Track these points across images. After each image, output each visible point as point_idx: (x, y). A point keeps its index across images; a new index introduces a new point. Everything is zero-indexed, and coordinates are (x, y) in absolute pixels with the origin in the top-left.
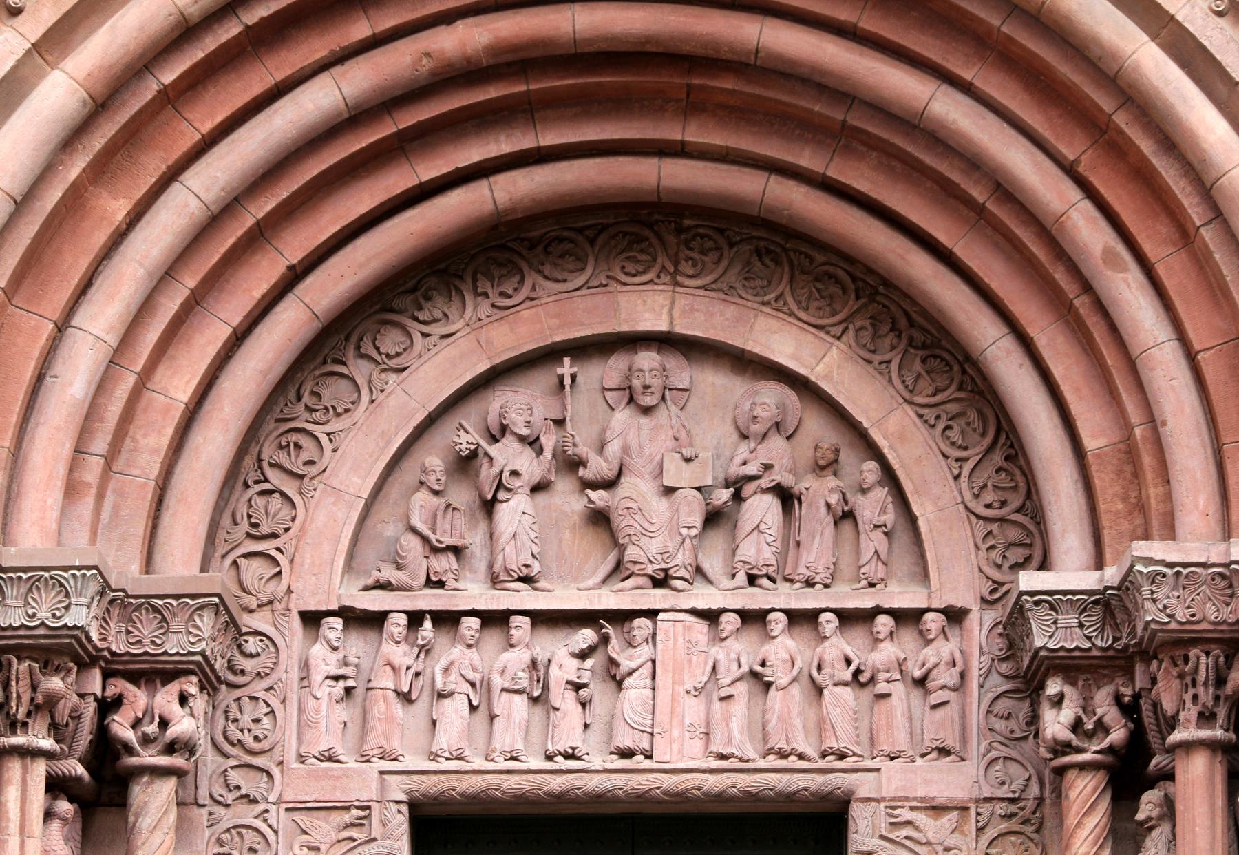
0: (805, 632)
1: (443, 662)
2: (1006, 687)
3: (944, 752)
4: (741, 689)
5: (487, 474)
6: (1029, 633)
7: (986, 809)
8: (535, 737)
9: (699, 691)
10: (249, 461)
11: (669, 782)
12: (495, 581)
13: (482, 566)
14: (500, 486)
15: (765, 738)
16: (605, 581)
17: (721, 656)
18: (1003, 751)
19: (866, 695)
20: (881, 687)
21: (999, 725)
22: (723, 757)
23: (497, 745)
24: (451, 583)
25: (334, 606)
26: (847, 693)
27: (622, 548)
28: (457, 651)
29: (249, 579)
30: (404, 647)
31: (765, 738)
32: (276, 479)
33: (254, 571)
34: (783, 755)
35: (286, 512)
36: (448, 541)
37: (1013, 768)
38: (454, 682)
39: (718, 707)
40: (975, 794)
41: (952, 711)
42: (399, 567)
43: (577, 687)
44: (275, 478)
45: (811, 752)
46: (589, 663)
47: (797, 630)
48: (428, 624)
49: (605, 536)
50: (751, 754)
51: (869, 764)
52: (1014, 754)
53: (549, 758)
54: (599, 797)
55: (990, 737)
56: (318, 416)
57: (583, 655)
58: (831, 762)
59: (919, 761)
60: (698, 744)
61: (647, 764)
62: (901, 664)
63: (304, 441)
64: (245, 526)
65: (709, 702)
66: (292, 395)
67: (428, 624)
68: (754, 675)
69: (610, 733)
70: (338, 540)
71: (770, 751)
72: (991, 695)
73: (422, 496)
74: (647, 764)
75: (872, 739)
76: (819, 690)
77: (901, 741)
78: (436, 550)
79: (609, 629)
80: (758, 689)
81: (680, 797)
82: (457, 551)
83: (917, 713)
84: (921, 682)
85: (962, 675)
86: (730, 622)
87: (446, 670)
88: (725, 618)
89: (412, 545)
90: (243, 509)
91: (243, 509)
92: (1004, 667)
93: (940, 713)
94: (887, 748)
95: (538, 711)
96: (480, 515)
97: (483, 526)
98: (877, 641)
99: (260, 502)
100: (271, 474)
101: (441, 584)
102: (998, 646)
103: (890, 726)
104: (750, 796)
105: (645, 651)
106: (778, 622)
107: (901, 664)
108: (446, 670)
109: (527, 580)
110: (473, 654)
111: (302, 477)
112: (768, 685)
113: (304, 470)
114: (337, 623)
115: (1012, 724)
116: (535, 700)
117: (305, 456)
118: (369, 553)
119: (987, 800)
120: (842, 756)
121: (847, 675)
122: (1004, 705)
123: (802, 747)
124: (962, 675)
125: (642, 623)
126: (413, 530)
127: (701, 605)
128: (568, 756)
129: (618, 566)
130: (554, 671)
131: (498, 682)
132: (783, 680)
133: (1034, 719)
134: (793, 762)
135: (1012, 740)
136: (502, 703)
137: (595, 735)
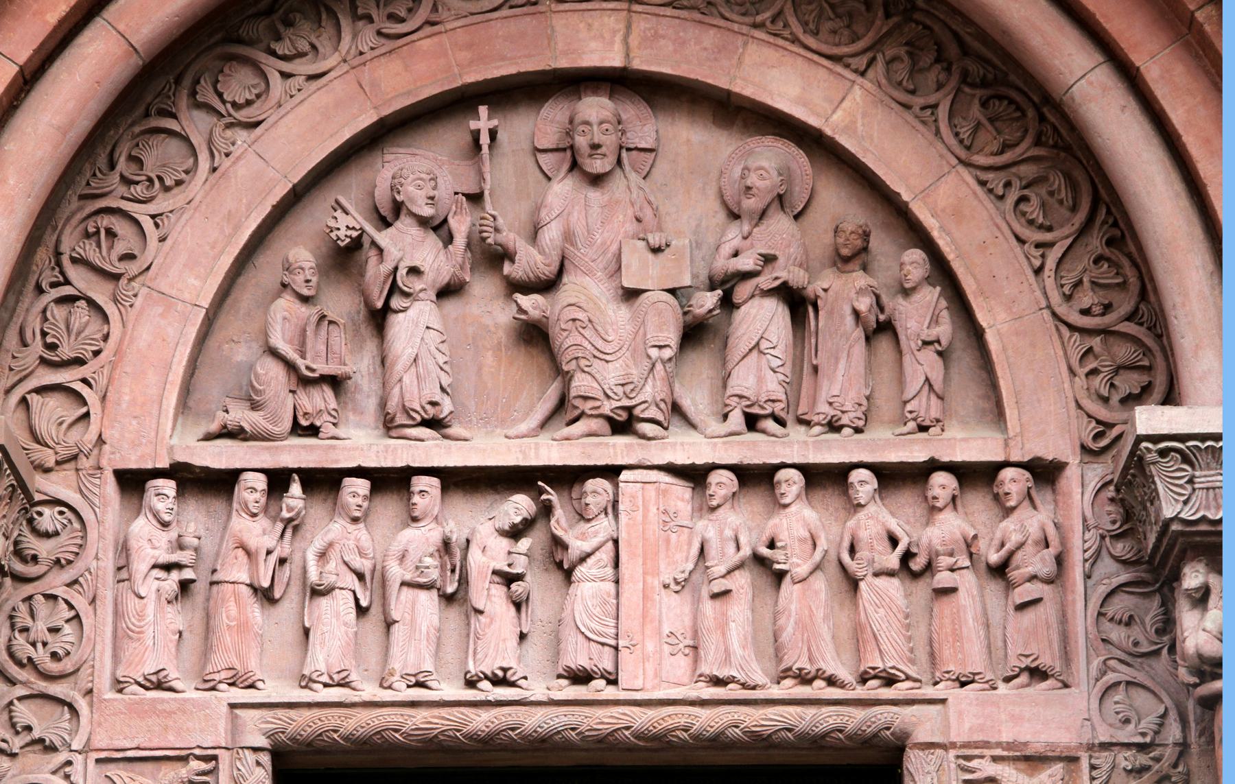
0: (829, 498)
1: (318, 544)
2: (1124, 577)
3: (1037, 674)
4: (742, 582)
5: (375, 272)
6: (1154, 497)
7: (1104, 759)
8: (451, 653)
9: (682, 585)
10: (43, 255)
11: (642, 719)
12: (389, 426)
13: (371, 404)
14: (394, 289)
15: (778, 655)
16: (544, 425)
17: (711, 534)
18: (1125, 673)
19: (922, 589)
20: (943, 579)
21: (1117, 634)
22: (718, 682)
23: (396, 664)
24: (327, 429)
25: (164, 464)
26: (893, 587)
27: (567, 378)
28: (338, 528)
29: (44, 426)
30: (262, 522)
31: (778, 655)
32: (80, 279)
33: (51, 411)
34: (804, 679)
35: (95, 328)
36: (322, 368)
37: (1141, 699)
38: (333, 573)
39: (708, 607)
40: (1086, 738)
41: (1046, 612)
42: (255, 406)
43: (509, 579)
44: (80, 279)
45: (844, 674)
46: (524, 544)
47: (818, 495)
48: (296, 488)
49: (543, 360)
50: (759, 677)
51: (929, 692)
52: (1141, 677)
53: (471, 684)
54: (543, 742)
55: (1103, 650)
56: (139, 191)
57: (515, 533)
58: (873, 689)
59: (1003, 688)
60: (681, 665)
61: (610, 692)
62: (969, 545)
63: (120, 226)
64: (37, 348)
65: (697, 601)
66: (102, 161)
67: (296, 488)
68: (759, 560)
69: (556, 644)
70: (169, 367)
71: (785, 674)
72: (1103, 590)
73: (285, 305)
74: (610, 692)
75: (932, 655)
76: (853, 583)
77: (974, 659)
78: (306, 382)
79: (552, 495)
80: (765, 581)
81: (659, 741)
82: (335, 382)
83: (996, 616)
84: (1000, 571)
85: (1060, 560)
86: (722, 482)
87: (323, 555)
88: (715, 477)
89: (273, 372)
90: (34, 324)
91: (34, 324)
92: (1120, 548)
93: (1030, 615)
94: (955, 668)
95: (454, 613)
96: (367, 331)
97: (371, 346)
98: (934, 510)
99: (59, 313)
100: (73, 272)
101: (313, 431)
102: (1109, 517)
103: (957, 636)
104: (760, 741)
105: (603, 527)
106: (791, 483)
107: (969, 545)
108: (323, 555)
109: (434, 424)
110: (360, 533)
111: (116, 277)
112: (780, 576)
113: (119, 268)
114: (168, 487)
115: (1136, 632)
116: (448, 599)
117: (120, 248)
118: (211, 387)
119: (1105, 746)
120: (890, 681)
121: (893, 561)
122: (1122, 604)
123: (832, 667)
124: (1060, 560)
125: (597, 488)
126: (274, 353)
127: (681, 459)
128: (500, 681)
129: (562, 403)
130: (475, 556)
131: (397, 573)
132: (802, 569)
133: (1168, 624)
134: (819, 689)
135: (1135, 656)
136: (402, 603)
137: (536, 650)
